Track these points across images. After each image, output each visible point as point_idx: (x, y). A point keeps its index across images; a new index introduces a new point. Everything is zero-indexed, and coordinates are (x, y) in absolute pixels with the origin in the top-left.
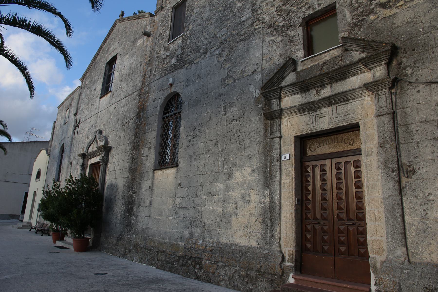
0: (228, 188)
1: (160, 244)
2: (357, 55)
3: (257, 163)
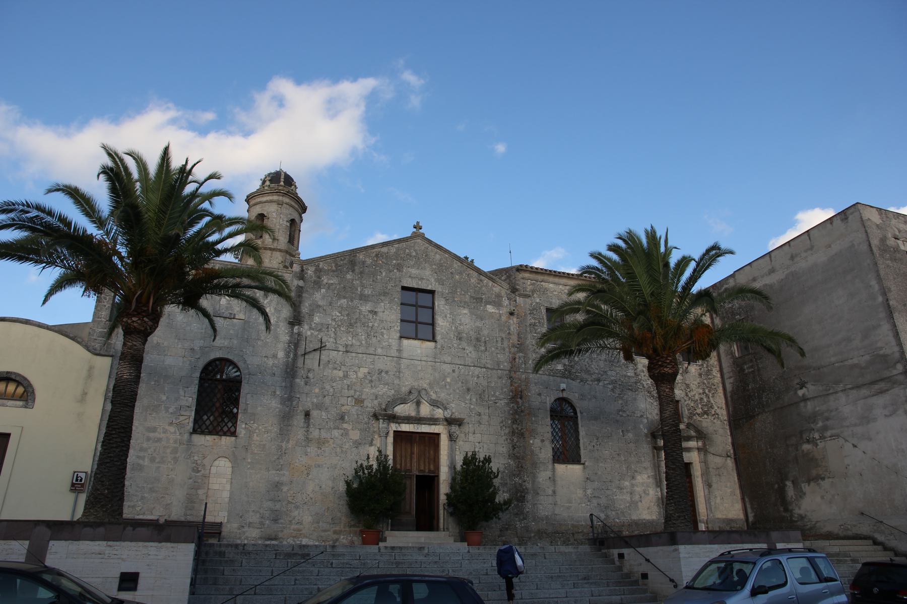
0: (633, 485)
1: (573, 526)
2: (693, 433)
3: (650, 472)
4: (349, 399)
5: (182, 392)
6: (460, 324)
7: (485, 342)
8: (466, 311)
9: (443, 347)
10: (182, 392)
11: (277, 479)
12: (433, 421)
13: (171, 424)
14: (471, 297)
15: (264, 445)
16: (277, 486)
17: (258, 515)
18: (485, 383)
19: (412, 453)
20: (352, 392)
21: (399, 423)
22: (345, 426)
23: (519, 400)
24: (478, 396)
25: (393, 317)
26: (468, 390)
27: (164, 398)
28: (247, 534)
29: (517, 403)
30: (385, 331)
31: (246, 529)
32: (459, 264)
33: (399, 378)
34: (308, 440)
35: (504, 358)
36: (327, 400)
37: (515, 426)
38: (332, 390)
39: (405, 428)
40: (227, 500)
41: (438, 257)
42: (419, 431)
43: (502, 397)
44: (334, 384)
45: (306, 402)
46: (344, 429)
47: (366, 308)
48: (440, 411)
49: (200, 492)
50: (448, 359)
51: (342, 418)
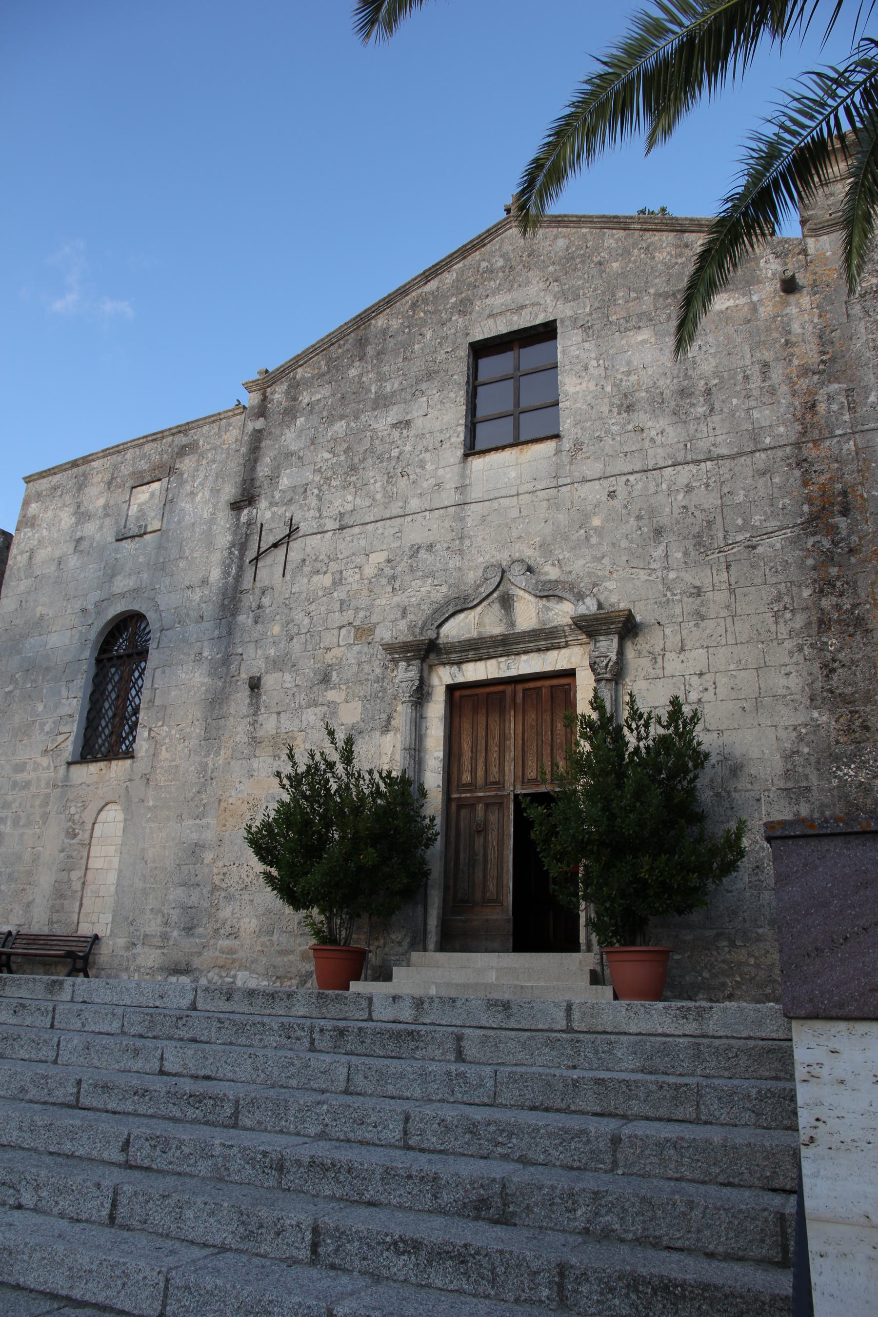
4: (344, 631)
5: (64, 693)
6: (628, 373)
7: (708, 392)
8: (645, 335)
9: (578, 446)
10: (64, 693)
11: (194, 836)
12: (546, 638)
13: (46, 752)
14: (658, 295)
15: (177, 766)
16: (195, 851)
17: (159, 919)
18: (711, 500)
19: (503, 738)
20: (349, 615)
21: (459, 663)
22: (332, 695)
23: (842, 522)
24: (689, 544)
25: (446, 418)
26: (658, 532)
27: (40, 708)
28: (140, 961)
29: (833, 530)
30: (427, 456)
31: (139, 949)
32: (622, 233)
33: (461, 552)
34: (255, 741)
35: (775, 420)
36: (296, 645)
37: (826, 603)
38: (307, 621)
39: (476, 671)
40: (113, 889)
41: (561, 243)
42: (513, 672)
43: (774, 524)
44: (313, 607)
45: (253, 661)
46: (329, 704)
47: (383, 422)
49: (75, 875)
50: (593, 468)
51: (325, 679)
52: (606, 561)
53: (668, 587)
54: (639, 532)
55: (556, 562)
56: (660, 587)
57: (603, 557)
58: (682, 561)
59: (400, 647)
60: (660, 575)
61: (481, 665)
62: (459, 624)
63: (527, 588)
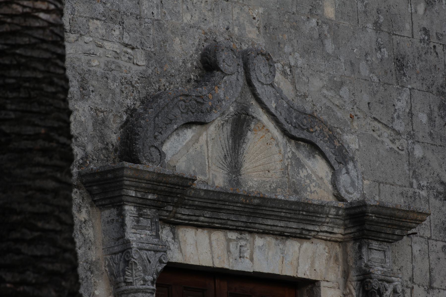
26: (400, 63)
42: (245, 266)
48: (318, 168)
52: (345, 91)
53: (414, 172)
54: (379, 56)
55: (288, 70)
56: (406, 167)
57: (342, 84)
58: (427, 130)
59: (149, 181)
60: (405, 146)
61: (202, 236)
62: (187, 147)
63: (278, 115)
